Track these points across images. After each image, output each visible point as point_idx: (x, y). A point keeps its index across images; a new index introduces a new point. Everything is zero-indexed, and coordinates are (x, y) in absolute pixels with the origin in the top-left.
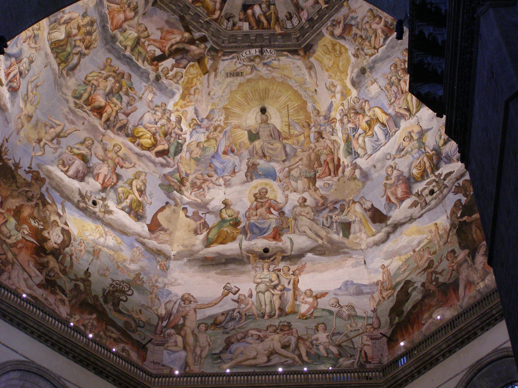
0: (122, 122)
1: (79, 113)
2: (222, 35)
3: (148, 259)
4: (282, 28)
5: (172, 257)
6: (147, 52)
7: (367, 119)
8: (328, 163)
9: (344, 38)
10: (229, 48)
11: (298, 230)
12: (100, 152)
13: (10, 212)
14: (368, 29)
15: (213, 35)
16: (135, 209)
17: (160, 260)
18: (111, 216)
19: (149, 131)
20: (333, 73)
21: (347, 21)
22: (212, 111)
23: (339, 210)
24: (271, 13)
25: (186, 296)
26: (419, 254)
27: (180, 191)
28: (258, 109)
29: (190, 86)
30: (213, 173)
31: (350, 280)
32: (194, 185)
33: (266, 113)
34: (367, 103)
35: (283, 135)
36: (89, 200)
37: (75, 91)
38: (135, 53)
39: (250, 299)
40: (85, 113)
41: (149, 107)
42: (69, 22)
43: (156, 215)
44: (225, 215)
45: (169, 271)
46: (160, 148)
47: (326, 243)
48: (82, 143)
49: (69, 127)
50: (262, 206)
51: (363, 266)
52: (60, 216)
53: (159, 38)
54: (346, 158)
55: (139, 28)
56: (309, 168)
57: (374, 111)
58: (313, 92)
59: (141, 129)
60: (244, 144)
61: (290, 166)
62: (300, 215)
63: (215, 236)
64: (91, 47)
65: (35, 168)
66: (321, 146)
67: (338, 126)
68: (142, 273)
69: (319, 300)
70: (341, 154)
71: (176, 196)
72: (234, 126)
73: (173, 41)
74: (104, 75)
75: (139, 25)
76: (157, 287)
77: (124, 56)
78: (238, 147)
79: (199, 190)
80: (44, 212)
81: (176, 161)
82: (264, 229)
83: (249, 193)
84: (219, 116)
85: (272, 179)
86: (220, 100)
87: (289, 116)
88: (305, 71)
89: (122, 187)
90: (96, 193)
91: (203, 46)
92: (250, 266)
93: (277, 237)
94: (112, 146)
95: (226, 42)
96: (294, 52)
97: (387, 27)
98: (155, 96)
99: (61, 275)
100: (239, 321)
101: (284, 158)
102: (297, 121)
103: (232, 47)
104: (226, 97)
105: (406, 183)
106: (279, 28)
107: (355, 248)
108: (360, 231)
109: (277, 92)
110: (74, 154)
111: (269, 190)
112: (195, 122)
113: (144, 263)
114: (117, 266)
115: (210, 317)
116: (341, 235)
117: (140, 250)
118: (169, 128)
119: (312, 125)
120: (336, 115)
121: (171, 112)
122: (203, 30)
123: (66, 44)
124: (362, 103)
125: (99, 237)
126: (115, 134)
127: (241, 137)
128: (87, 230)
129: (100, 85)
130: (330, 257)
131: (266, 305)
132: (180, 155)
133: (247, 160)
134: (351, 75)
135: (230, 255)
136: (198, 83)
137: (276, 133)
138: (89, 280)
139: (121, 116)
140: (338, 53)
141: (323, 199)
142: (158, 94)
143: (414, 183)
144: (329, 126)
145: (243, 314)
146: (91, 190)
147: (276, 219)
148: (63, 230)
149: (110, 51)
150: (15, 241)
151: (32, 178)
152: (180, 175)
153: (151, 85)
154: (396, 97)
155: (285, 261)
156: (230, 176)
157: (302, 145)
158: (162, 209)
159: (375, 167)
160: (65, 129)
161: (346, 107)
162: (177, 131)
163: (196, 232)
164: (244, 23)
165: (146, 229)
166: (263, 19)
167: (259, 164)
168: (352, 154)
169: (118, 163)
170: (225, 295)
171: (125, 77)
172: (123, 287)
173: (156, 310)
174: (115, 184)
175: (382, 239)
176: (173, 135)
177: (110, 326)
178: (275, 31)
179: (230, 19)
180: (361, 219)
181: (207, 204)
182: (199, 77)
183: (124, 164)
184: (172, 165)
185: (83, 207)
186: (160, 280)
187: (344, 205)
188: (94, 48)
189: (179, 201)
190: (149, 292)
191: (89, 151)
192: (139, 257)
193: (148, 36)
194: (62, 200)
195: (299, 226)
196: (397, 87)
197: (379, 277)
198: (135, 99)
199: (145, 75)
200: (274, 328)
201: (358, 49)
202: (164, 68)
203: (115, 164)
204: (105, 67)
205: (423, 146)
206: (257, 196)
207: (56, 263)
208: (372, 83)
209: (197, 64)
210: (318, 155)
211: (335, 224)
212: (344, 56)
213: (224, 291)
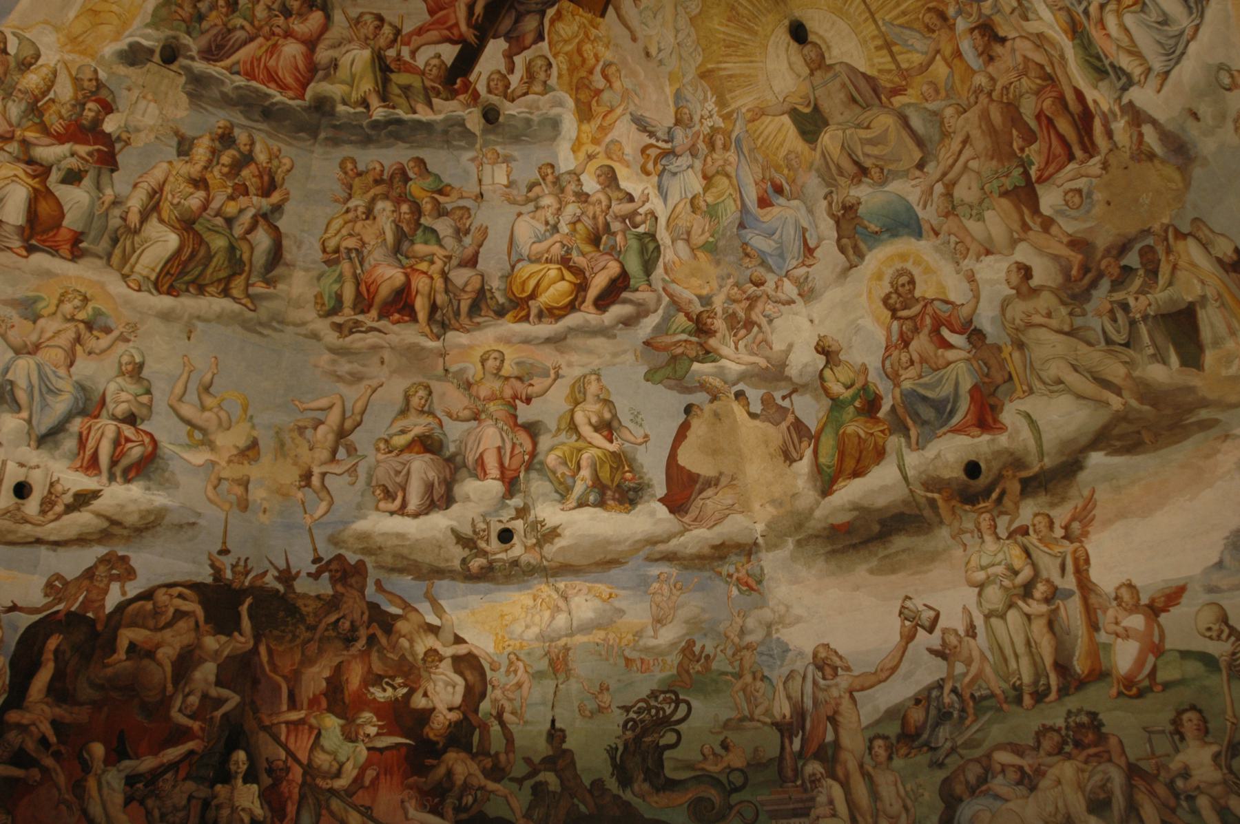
0: (469, 289)
1: (358, 345)
5: (760, 541)
6: (423, 73)
8: (1050, 122)
11: (1040, 379)
13: (319, 704)
16: (612, 481)
17: (732, 570)
18: (560, 543)
19: (547, 261)
22: (678, 96)
23: (1141, 272)
25: (823, 654)
27: (708, 355)
29: (583, 74)
30: (761, 272)
33: (812, 38)
35: (885, 82)
36: (487, 542)
37: (319, 296)
38: (395, 98)
40: (370, 334)
42: (158, 203)
45: (765, 583)
46: (599, 283)
48: (404, 412)
49: (353, 395)
50: (916, 330)
52: (434, 630)
53: (427, 17)
54: (1096, 87)
55: (363, 31)
59: (526, 270)
61: (945, 174)
62: (1031, 325)
64: (278, 178)
65: (327, 553)
66: (1008, 70)
68: (695, 637)
69: (1163, 618)
70: (1077, 75)
72: (749, 115)
74: (361, 209)
75: (357, 22)
76: (747, 647)
77: (376, 125)
78: (786, 171)
79: (749, 332)
80: (394, 647)
82: (946, 400)
86: (681, 58)
87: (872, 15)
89: (552, 449)
90: (496, 511)
92: (944, 532)
93: (990, 420)
94: (479, 366)
98: (513, 164)
99: (491, 785)
100: (962, 719)
101: (917, 155)
102: (901, 21)
110: (402, 451)
111: (916, 272)
112: (653, 152)
113: (692, 605)
114: (622, 662)
115: (891, 714)
116: (1174, 360)
117: (668, 578)
118: (594, 217)
119: (951, 11)
121: (576, 175)
123: (201, 241)
125: (553, 617)
126: (468, 331)
127: (780, 138)
129: (366, 239)
131: (1017, 656)
132: (661, 263)
135: (887, 508)
136: (601, 49)
137: (862, 84)
139: (460, 276)
142: (516, 154)
145: (967, 696)
146: (482, 510)
147: (968, 360)
148: (457, 660)
149: (335, 142)
150: (355, 772)
151: (334, 581)
152: (687, 315)
153: (486, 144)
157: (951, 92)
158: (682, 433)
159: (1195, 116)
160: (349, 406)
162: (617, 208)
163: (789, 457)
165: (662, 511)
167: (859, 203)
168: (1107, 73)
170: (909, 637)
171: (411, 175)
172: (658, 710)
174: (533, 454)
176: (616, 226)
180: (1220, 295)
181: (783, 365)
182: (594, 31)
184: (652, 307)
185: (482, 568)
186: (751, 623)
187: (1150, 249)
188: (289, 171)
189: (717, 382)
190: (733, 675)
191: (430, 419)
192: (674, 598)
193: (398, 32)
194: (423, 586)
195: (1037, 365)
198: (468, 209)
199: (453, 134)
200: (1056, 737)
202: (489, 79)
204: (351, 187)
206: (891, 301)
207: (469, 762)
210: (1009, 104)
211: (1143, 329)
213: (903, 626)
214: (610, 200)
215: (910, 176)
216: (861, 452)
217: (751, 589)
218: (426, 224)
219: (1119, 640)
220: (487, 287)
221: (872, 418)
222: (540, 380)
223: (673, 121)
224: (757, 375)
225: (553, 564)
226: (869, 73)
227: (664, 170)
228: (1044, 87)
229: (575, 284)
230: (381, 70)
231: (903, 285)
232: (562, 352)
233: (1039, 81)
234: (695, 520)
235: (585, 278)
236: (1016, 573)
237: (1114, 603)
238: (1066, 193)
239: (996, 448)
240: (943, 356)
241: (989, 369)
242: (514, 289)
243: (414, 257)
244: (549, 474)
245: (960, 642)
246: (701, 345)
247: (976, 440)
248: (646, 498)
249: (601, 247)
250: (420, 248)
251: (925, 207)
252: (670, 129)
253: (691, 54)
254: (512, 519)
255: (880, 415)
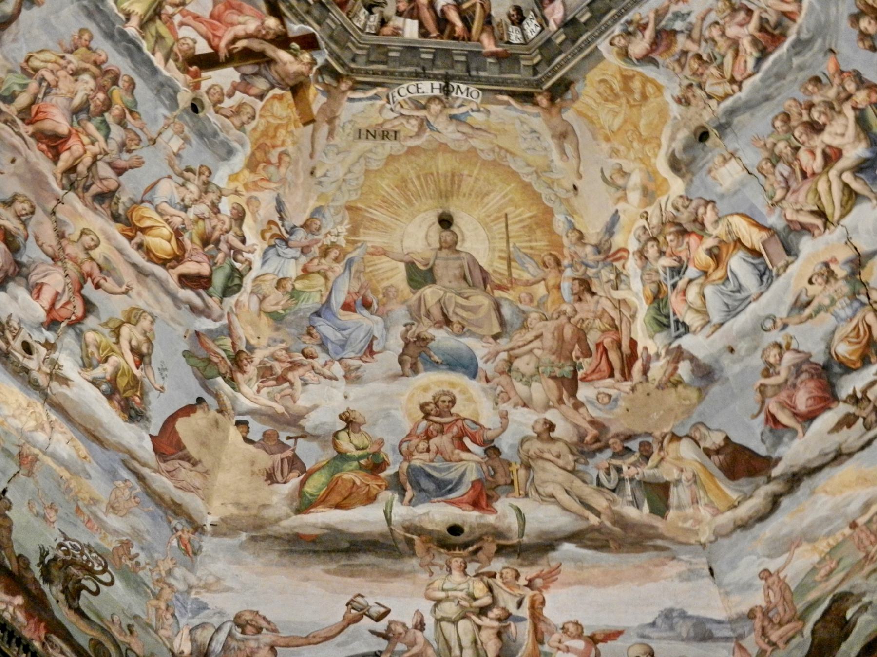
0: (105, 182)
2: (353, 43)
3: (153, 517)
4: (499, 40)
5: (208, 528)
6: (178, 40)
7: (709, 243)
8: (605, 351)
9: (655, 63)
10: (367, 73)
11: (537, 491)
12: (49, 238)
14: (717, 39)
15: (331, 37)
17: (179, 527)
18: (64, 389)
20: (622, 144)
21: (663, 23)
22: (318, 211)
23: (638, 454)
24: (474, 5)
25: (248, 617)
26: (868, 528)
28: (432, 218)
29: (268, 142)
30: (316, 350)
31: (678, 607)
32: (265, 372)
33: (454, 228)
34: (710, 207)
35: (495, 279)
36: (14, 337)
39: (419, 633)
41: (172, 167)
43: (172, 419)
44: (346, 444)
45: (199, 558)
46: (189, 267)
47: (608, 524)
50: (442, 432)
51: (708, 580)
53: (206, 15)
54: (652, 337)
56: (560, 356)
57: (729, 224)
58: (567, 191)
59: (147, 210)
60: (397, 291)
61: (512, 349)
63: (320, 489)
66: (589, 311)
67: (632, 266)
68: (135, 543)
69: (600, 646)
71: (222, 390)
72: (371, 250)
73: (239, 30)
74: (71, 66)
76: (170, 586)
77: (123, 34)
78: (381, 296)
79: (278, 384)
81: (227, 310)
82: (450, 482)
83: (410, 399)
84: (336, 224)
85: (465, 373)
86: (339, 188)
88: (550, 143)
89: (94, 330)
90: (32, 327)
91: (306, 57)
92: (414, 562)
93: (484, 503)
94: (78, 233)
95: (362, 60)
96: (527, 98)
97: (766, 31)
98: (187, 146)
101: (497, 329)
103: (375, 73)
104: (354, 183)
105: (819, 376)
106: (492, 42)
107: (682, 539)
108: (695, 501)
109: (481, 183)
112: (275, 230)
113: (143, 522)
114: (74, 507)
116: (646, 508)
117: (132, 488)
118: (214, 228)
119: (565, 262)
120: (626, 242)
121: (221, 194)
122: (309, 19)
124: (696, 209)
125: (35, 429)
126: (86, 205)
127: (389, 274)
128: (6, 403)
129: (61, 85)
130: (624, 556)
131: (461, 648)
133: (404, 328)
134: (669, 146)
135: (362, 535)
136: (289, 141)
138: (6, 517)
139: (104, 170)
140: (637, 96)
141: (596, 429)
143: (842, 375)
144: (608, 269)
146: (22, 316)
147: (479, 463)
149: (90, 15)
152: (233, 343)
153: (180, 117)
154: (788, 188)
155: (507, 555)
156: (360, 359)
157: (541, 304)
158: (187, 410)
159: (732, 350)
161: (655, 221)
163: (270, 477)
164: (409, 21)
165: (148, 445)
166: (453, 16)
167: (432, 339)
168: (669, 326)
169: (90, 275)
171: (121, 83)
172: (88, 561)
173: (168, 638)
174: (79, 321)
175: (757, 511)
176: (223, 246)
177: (58, 636)
178: (483, 47)
179: (375, 10)
180: (694, 476)
181: (302, 417)
183: (102, 281)
184: (215, 315)
186: (178, 572)
187: (649, 444)
189: (228, 403)
190: (152, 591)
191: (21, 227)
192: (130, 504)
195: (537, 482)
196: (790, 165)
197: (758, 599)
198: (140, 140)
201: (691, 85)
203: (82, 274)
204: (77, 48)
205: (863, 290)
206: (428, 408)
208: (725, 161)
209: (289, 95)
210: (581, 329)
211: (628, 486)
212: (653, 103)
213: (349, 612)
214: (231, 228)
215: (484, 339)
216: (351, 494)
217: (187, 552)
218: (107, 120)
219: (560, 652)
220: (117, 194)
221: (373, 474)
222: (114, 284)
223: (301, 223)
224: (269, 416)
225: (54, 398)
226: (486, 268)
227: (274, 246)
228: (608, 330)
229: (175, 253)
230: (155, 10)
231: (444, 401)
232: (139, 282)
233: (607, 326)
234: (168, 472)
235: (183, 255)
236: (475, 599)
237: (561, 631)
238: (599, 393)
239: (483, 521)
240: (458, 454)
241: (495, 473)
242: (134, 214)
243: (84, 129)
244: (83, 343)
245: (406, 632)
246: (231, 371)
247: (466, 513)
248: (142, 424)
249: (206, 249)
250: (91, 127)
251: (486, 362)
252: (295, 227)
253: (349, 191)
254: (40, 343)
255: (382, 475)
